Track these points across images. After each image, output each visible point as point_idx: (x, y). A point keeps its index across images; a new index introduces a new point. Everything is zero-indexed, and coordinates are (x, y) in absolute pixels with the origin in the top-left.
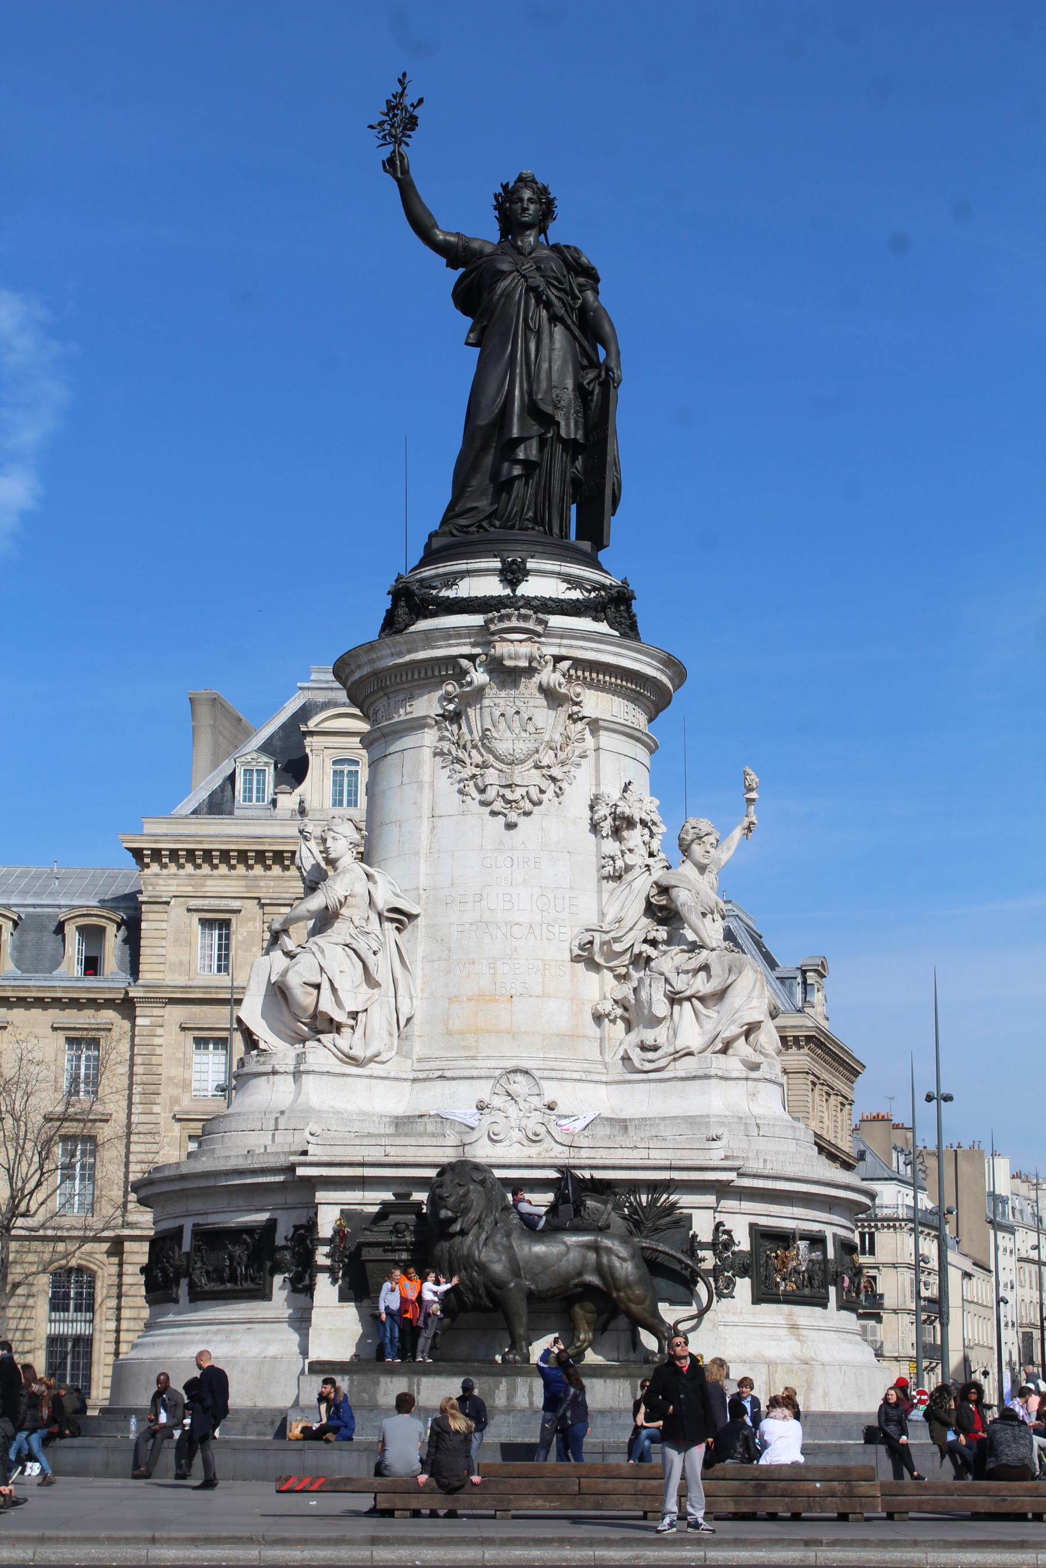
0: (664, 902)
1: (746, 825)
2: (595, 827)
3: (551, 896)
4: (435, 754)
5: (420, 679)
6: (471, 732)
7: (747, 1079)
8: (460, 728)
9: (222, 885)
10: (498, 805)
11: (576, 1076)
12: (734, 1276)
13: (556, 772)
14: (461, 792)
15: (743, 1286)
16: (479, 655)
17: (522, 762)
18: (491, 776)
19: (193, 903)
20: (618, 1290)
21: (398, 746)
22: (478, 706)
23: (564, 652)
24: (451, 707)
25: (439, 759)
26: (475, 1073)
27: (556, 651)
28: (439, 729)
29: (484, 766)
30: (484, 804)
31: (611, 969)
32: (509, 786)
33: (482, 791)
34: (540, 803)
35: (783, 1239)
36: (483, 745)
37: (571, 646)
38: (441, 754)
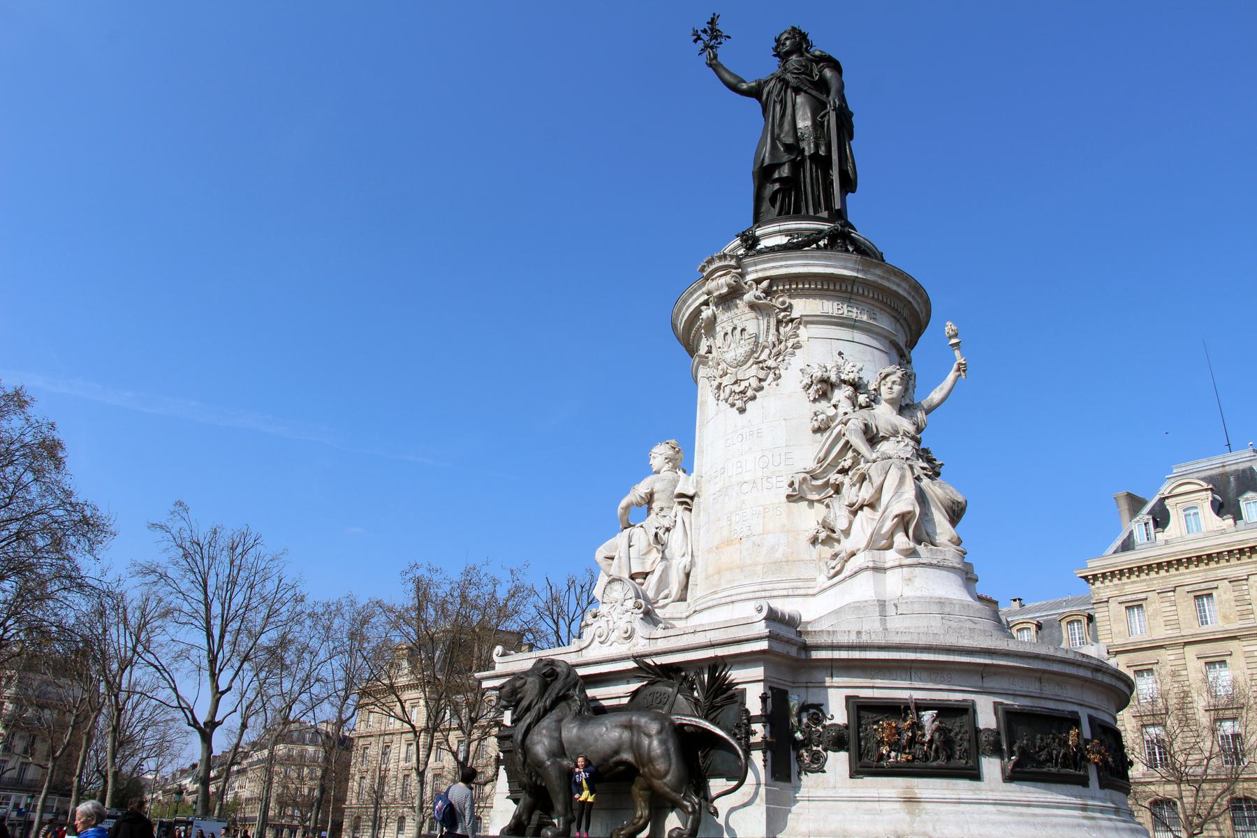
1: (955, 367)
3: (770, 456)
7: (901, 566)
9: (1133, 587)
10: (731, 400)
11: (785, 593)
12: (825, 750)
13: (771, 363)
15: (838, 761)
17: (745, 362)
18: (726, 381)
19: (1123, 599)
20: (644, 766)
23: (761, 275)
26: (710, 604)
27: (754, 276)
31: (819, 501)
32: (736, 382)
34: (761, 388)
35: (893, 709)
37: (765, 269)
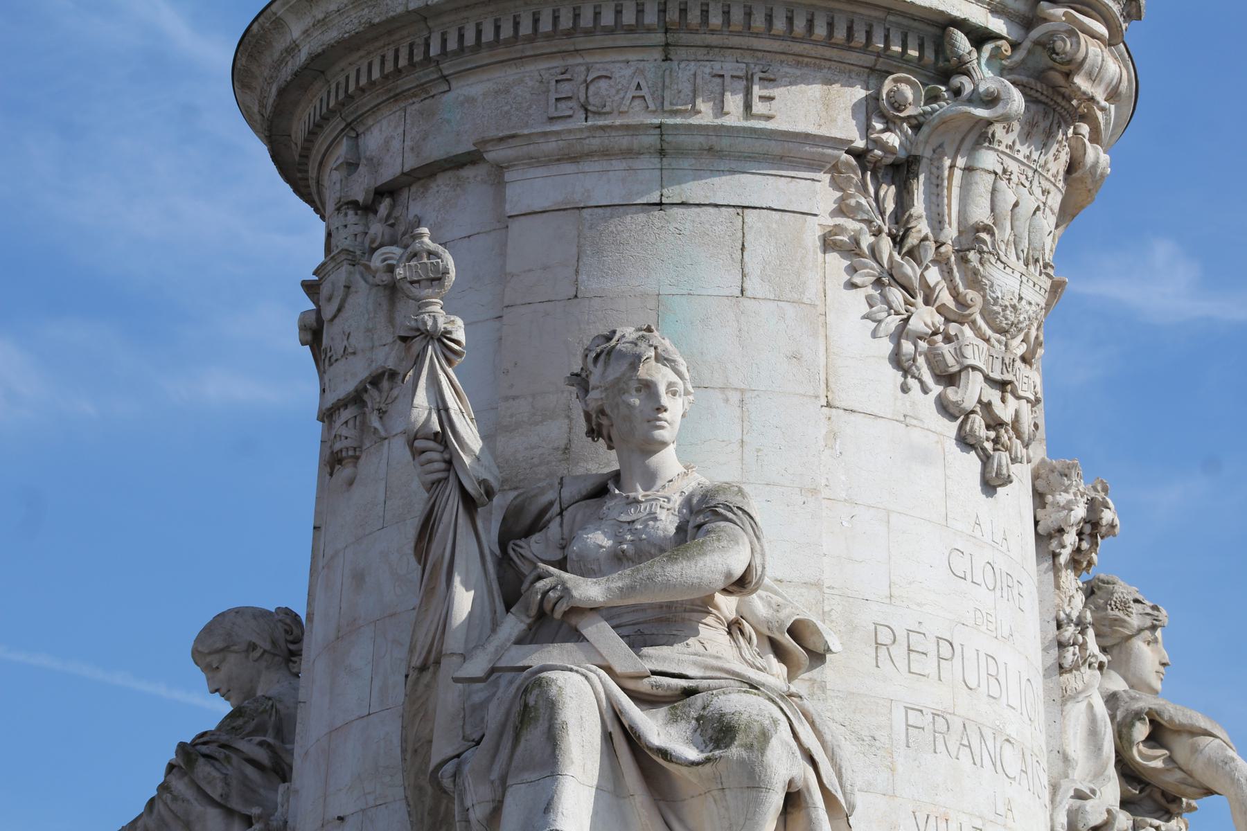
0: (1158, 764)
2: (1046, 538)
4: (828, 243)
5: (790, 35)
6: (937, 222)
8: (903, 201)
14: (897, 360)
16: (1002, 38)
21: (695, 190)
22: (961, 162)
24: (893, 139)
25: (837, 263)
28: (835, 184)
29: (959, 313)
30: (945, 408)
32: (1002, 385)
33: (950, 379)
36: (964, 260)
38: (852, 250)
